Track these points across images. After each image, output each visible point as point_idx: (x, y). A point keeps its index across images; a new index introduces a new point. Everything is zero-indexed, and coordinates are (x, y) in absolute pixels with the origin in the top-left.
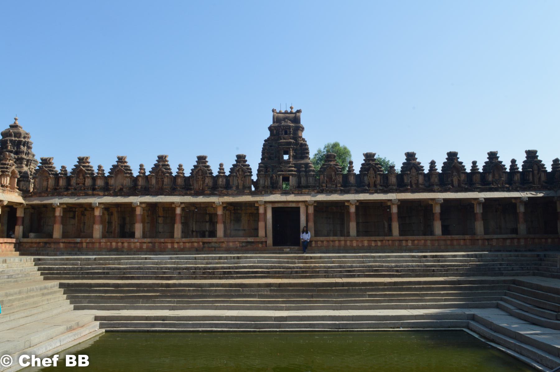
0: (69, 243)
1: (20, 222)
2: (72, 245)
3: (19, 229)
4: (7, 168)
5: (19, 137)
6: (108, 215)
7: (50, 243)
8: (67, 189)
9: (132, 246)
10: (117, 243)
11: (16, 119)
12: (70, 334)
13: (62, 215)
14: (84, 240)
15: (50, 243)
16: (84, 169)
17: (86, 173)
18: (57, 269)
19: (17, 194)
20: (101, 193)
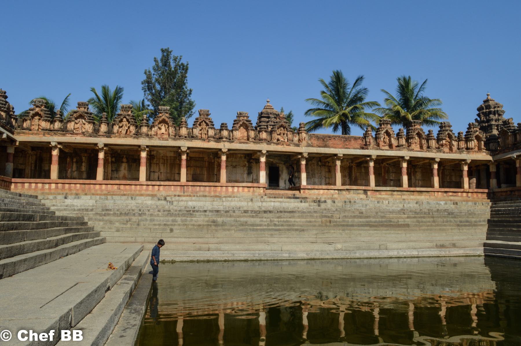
1: (493, 175)
4: (471, 134)
5: (490, 108)
7: (514, 191)
11: (488, 95)
15: (514, 191)
19: (484, 154)
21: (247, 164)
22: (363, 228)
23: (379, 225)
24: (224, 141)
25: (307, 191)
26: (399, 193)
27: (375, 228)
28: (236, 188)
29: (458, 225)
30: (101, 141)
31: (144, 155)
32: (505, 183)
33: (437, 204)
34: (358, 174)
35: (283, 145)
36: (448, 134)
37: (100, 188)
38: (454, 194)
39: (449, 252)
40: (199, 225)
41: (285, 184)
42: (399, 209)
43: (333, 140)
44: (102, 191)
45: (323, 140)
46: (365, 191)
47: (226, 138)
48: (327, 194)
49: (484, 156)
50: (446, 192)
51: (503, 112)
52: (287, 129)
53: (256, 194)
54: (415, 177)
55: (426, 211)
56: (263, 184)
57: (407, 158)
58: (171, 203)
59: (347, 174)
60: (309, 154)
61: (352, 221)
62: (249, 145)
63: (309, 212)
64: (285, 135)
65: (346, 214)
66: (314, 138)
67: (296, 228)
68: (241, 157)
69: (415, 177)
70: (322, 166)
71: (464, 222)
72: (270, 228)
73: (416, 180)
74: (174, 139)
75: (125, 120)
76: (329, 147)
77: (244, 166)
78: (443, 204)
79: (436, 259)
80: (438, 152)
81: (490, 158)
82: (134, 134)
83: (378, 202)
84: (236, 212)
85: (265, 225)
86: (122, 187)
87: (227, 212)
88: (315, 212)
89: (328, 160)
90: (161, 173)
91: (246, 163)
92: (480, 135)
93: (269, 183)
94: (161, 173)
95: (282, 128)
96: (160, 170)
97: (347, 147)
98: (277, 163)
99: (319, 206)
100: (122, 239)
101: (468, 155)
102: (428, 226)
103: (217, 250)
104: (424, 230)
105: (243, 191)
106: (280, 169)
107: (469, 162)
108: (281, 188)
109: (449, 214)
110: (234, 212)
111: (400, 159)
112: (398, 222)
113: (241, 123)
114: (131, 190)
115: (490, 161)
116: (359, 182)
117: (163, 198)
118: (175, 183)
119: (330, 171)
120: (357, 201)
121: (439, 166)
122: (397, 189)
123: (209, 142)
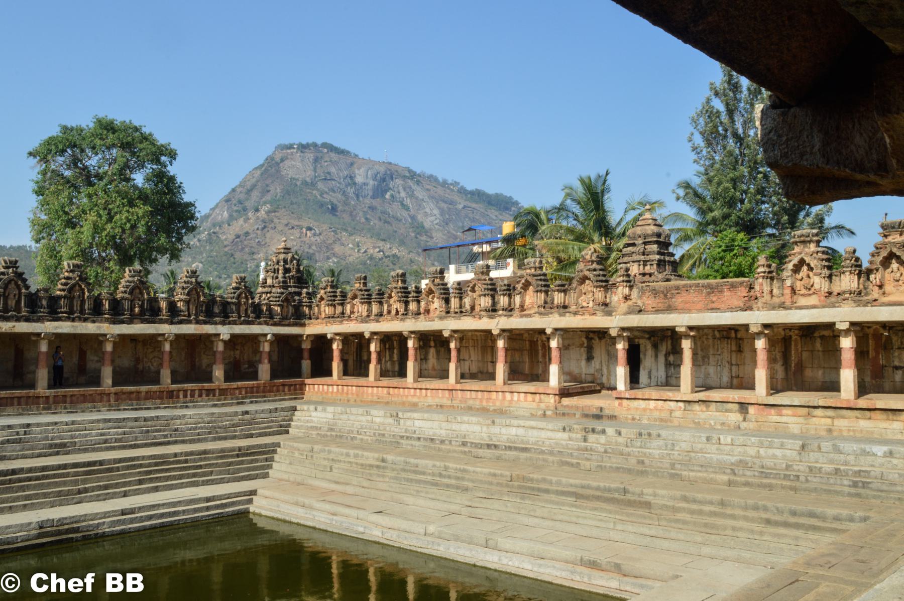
12: (586, 571)
21: (585, 341)
24: (500, 316)
25: (625, 402)
26: (830, 412)
30: (366, 329)
34: (805, 355)
37: (372, 392)
41: (650, 378)
42: (734, 459)
43: (684, 294)
45: (666, 296)
46: (743, 406)
56: (553, 389)
59: (779, 356)
62: (533, 319)
71: (802, 515)
74: (441, 318)
77: (582, 345)
96: (470, 357)
105: (526, 401)
106: (642, 348)
108: (642, 386)
119: (740, 350)
123: (480, 318)
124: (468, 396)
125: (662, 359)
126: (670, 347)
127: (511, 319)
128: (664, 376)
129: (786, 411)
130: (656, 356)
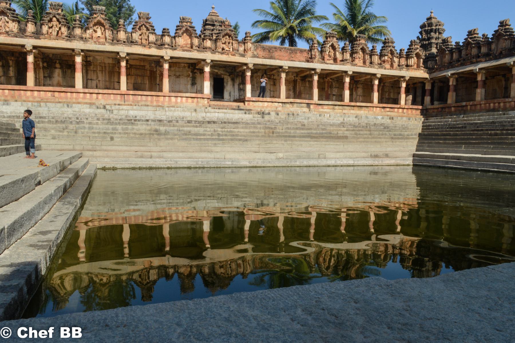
0: (458, 106)
1: (427, 93)
2: (460, 108)
3: (427, 99)
6: (505, 81)
8: (458, 61)
9: (508, 105)
10: (494, 103)
11: (431, 12)
13: (454, 84)
14: (468, 103)
16: (470, 40)
17: (472, 44)
18: (434, 125)
19: (422, 71)
20: (483, 60)
21: (191, 74)
22: (304, 139)
23: (320, 136)
24: (166, 48)
25: (251, 103)
26: (341, 107)
27: (316, 139)
28: (179, 99)
29: (392, 138)
30: (29, 43)
31: (78, 60)
32: (437, 101)
33: (375, 118)
34: (302, 88)
35: (228, 54)
36: (391, 50)
37: (32, 95)
38: (391, 110)
39: (382, 161)
40: (141, 134)
41: (230, 96)
42: (339, 122)
43: (279, 51)
44: (34, 98)
45: (269, 51)
46: (308, 105)
47: (168, 45)
48: (271, 107)
49: (421, 74)
50: (384, 108)
51: (444, 30)
52: (232, 37)
53: (200, 105)
54: (357, 93)
55: (364, 124)
56: (208, 95)
57: (350, 73)
58: (111, 111)
60: (254, 65)
61: (294, 133)
63: (253, 124)
64: (231, 44)
65: (289, 126)
66: (260, 49)
67: (240, 138)
68: (184, 67)
69: (357, 93)
70: (266, 78)
71: (397, 135)
72: (214, 137)
73: (357, 95)
75: (54, 19)
76: (275, 59)
77: (188, 76)
78: (380, 119)
79: (370, 168)
80: (379, 68)
81: (426, 76)
82: (67, 36)
83: (320, 115)
84: (179, 122)
85: (209, 135)
86: (56, 94)
87: (170, 121)
88: (259, 123)
89: (274, 72)
90: (99, 81)
91: (190, 73)
92: (420, 52)
93: (214, 95)
94: (99, 81)
95: (227, 37)
96: (97, 77)
97: (292, 59)
98: (222, 74)
99: (263, 118)
100: (59, 147)
101: (407, 72)
102: (365, 138)
103: (160, 157)
104: (361, 142)
105: (187, 102)
106: (225, 80)
107: (407, 78)
108: (226, 100)
109: (385, 128)
110: (177, 121)
111: (344, 74)
112: (338, 134)
113: (184, 29)
114: (67, 98)
115: (427, 78)
116: (303, 96)
117: (102, 107)
118: (115, 92)
119: (274, 84)
120: (300, 114)
121: (379, 82)
122: (339, 103)
123: (150, 48)
124: (139, 99)
125: (236, 86)
126: (240, 81)
127: (175, 51)
128: (238, 95)
129: (325, 107)
130: (234, 85)
